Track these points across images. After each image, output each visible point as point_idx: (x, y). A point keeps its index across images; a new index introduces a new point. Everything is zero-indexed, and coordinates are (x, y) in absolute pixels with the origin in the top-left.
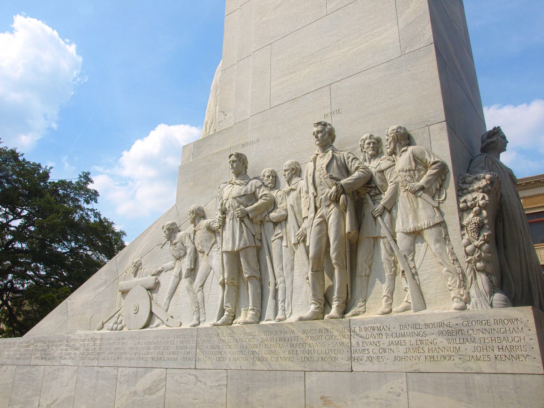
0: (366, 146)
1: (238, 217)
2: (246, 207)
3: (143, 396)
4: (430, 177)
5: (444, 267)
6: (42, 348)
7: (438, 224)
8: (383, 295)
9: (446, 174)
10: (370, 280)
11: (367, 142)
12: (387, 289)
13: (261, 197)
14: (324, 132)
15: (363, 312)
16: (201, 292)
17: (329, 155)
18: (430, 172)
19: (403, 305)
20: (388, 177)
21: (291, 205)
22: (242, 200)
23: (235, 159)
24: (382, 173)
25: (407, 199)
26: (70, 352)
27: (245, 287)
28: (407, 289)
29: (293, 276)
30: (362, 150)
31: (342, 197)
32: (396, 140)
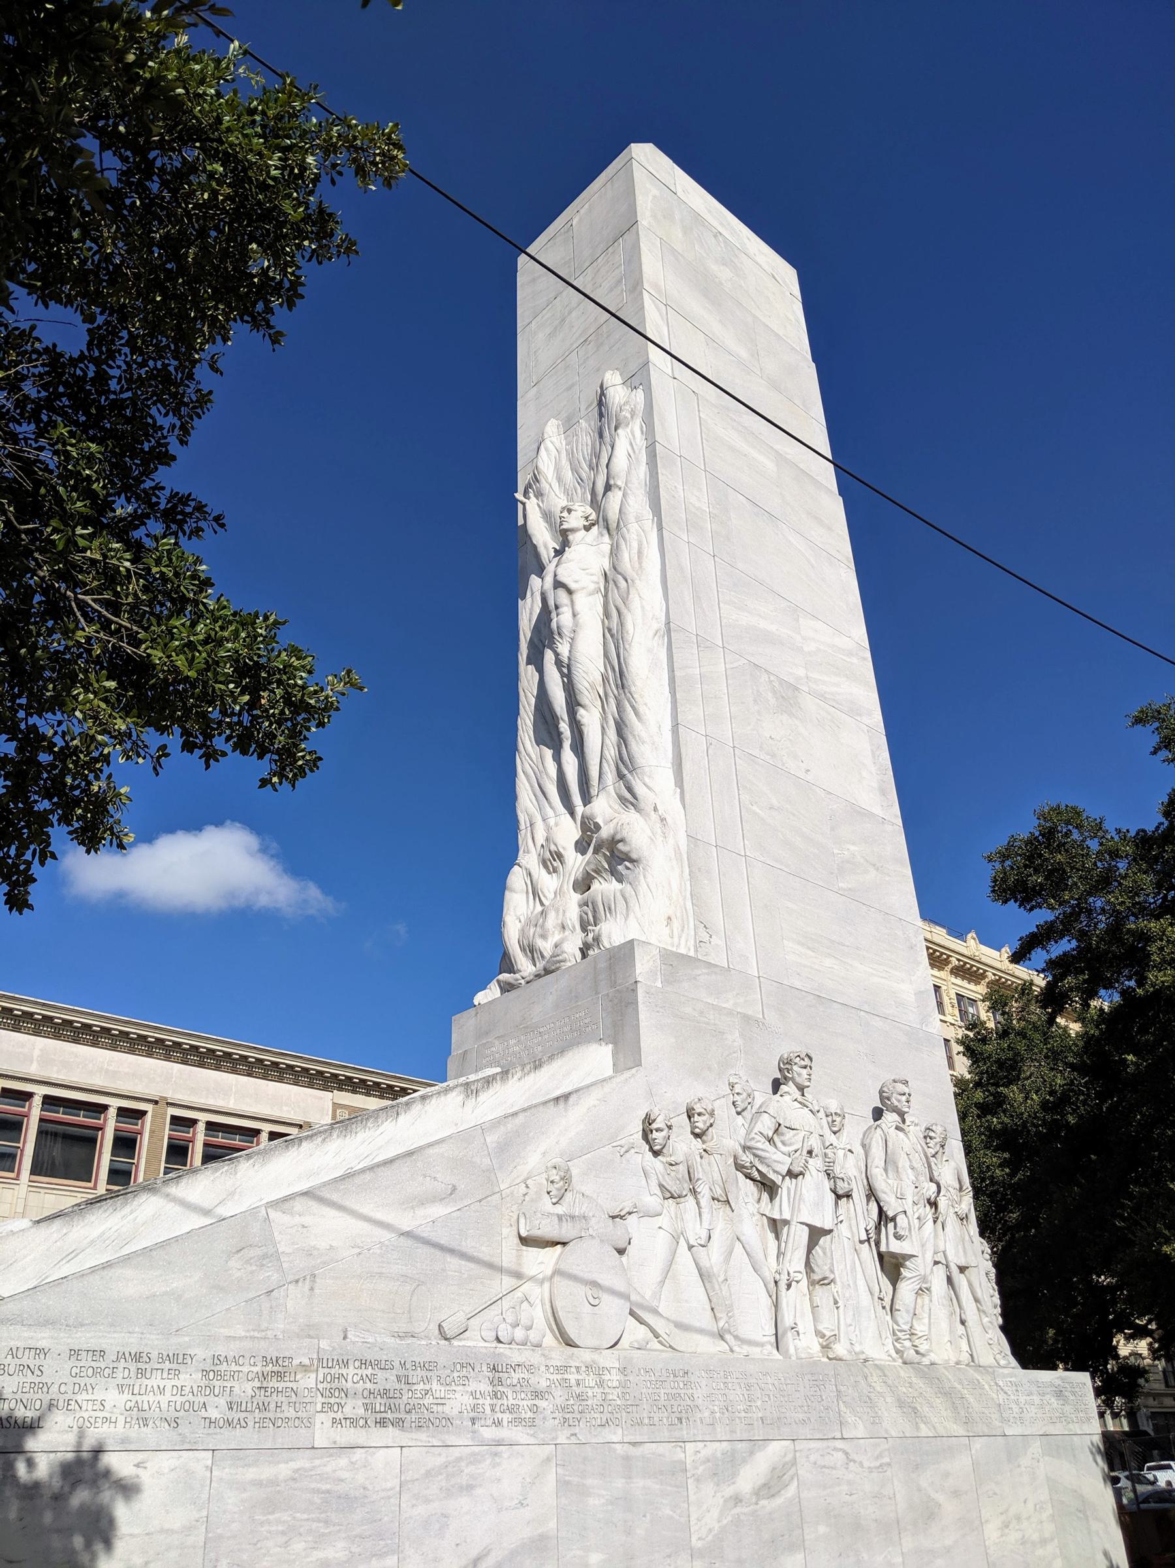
3: (757, 1504)
6: (369, 1385)
26: (514, 1402)
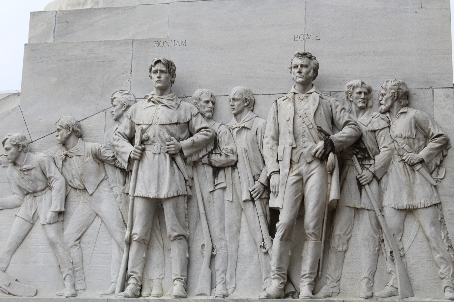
0: (355, 95)
1: (167, 152)
2: (179, 140)
4: (432, 151)
5: (438, 253)
7: (435, 205)
8: (363, 277)
9: (447, 150)
10: (346, 258)
11: (358, 90)
12: (369, 270)
13: (199, 130)
14: (309, 68)
15: (337, 294)
16: (78, 247)
17: (315, 99)
18: (432, 145)
19: (388, 289)
20: (381, 140)
21: (245, 148)
22: (174, 129)
23: (164, 68)
24: (373, 133)
25: (403, 170)
27: (161, 248)
28: (392, 272)
29: (239, 241)
30: (347, 98)
31: (331, 156)
32: (396, 98)
